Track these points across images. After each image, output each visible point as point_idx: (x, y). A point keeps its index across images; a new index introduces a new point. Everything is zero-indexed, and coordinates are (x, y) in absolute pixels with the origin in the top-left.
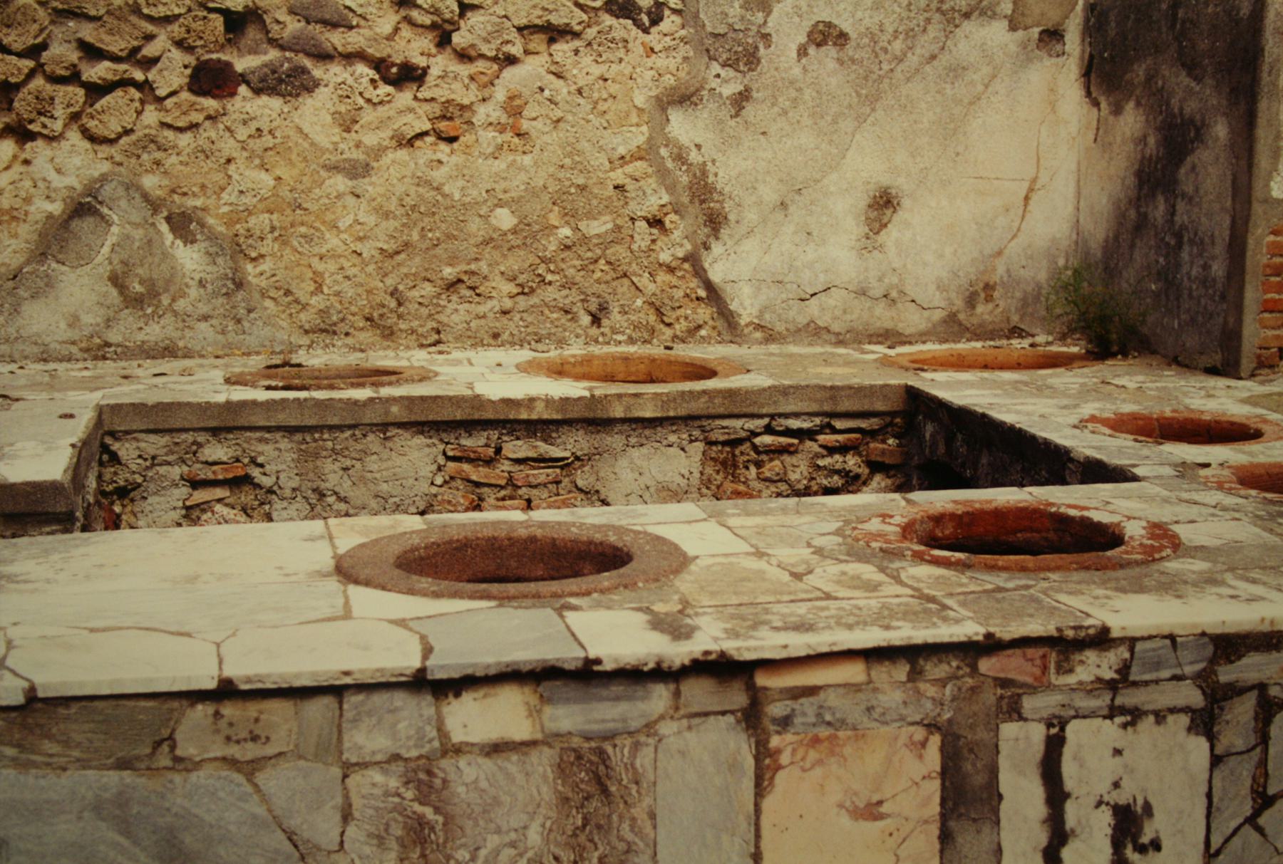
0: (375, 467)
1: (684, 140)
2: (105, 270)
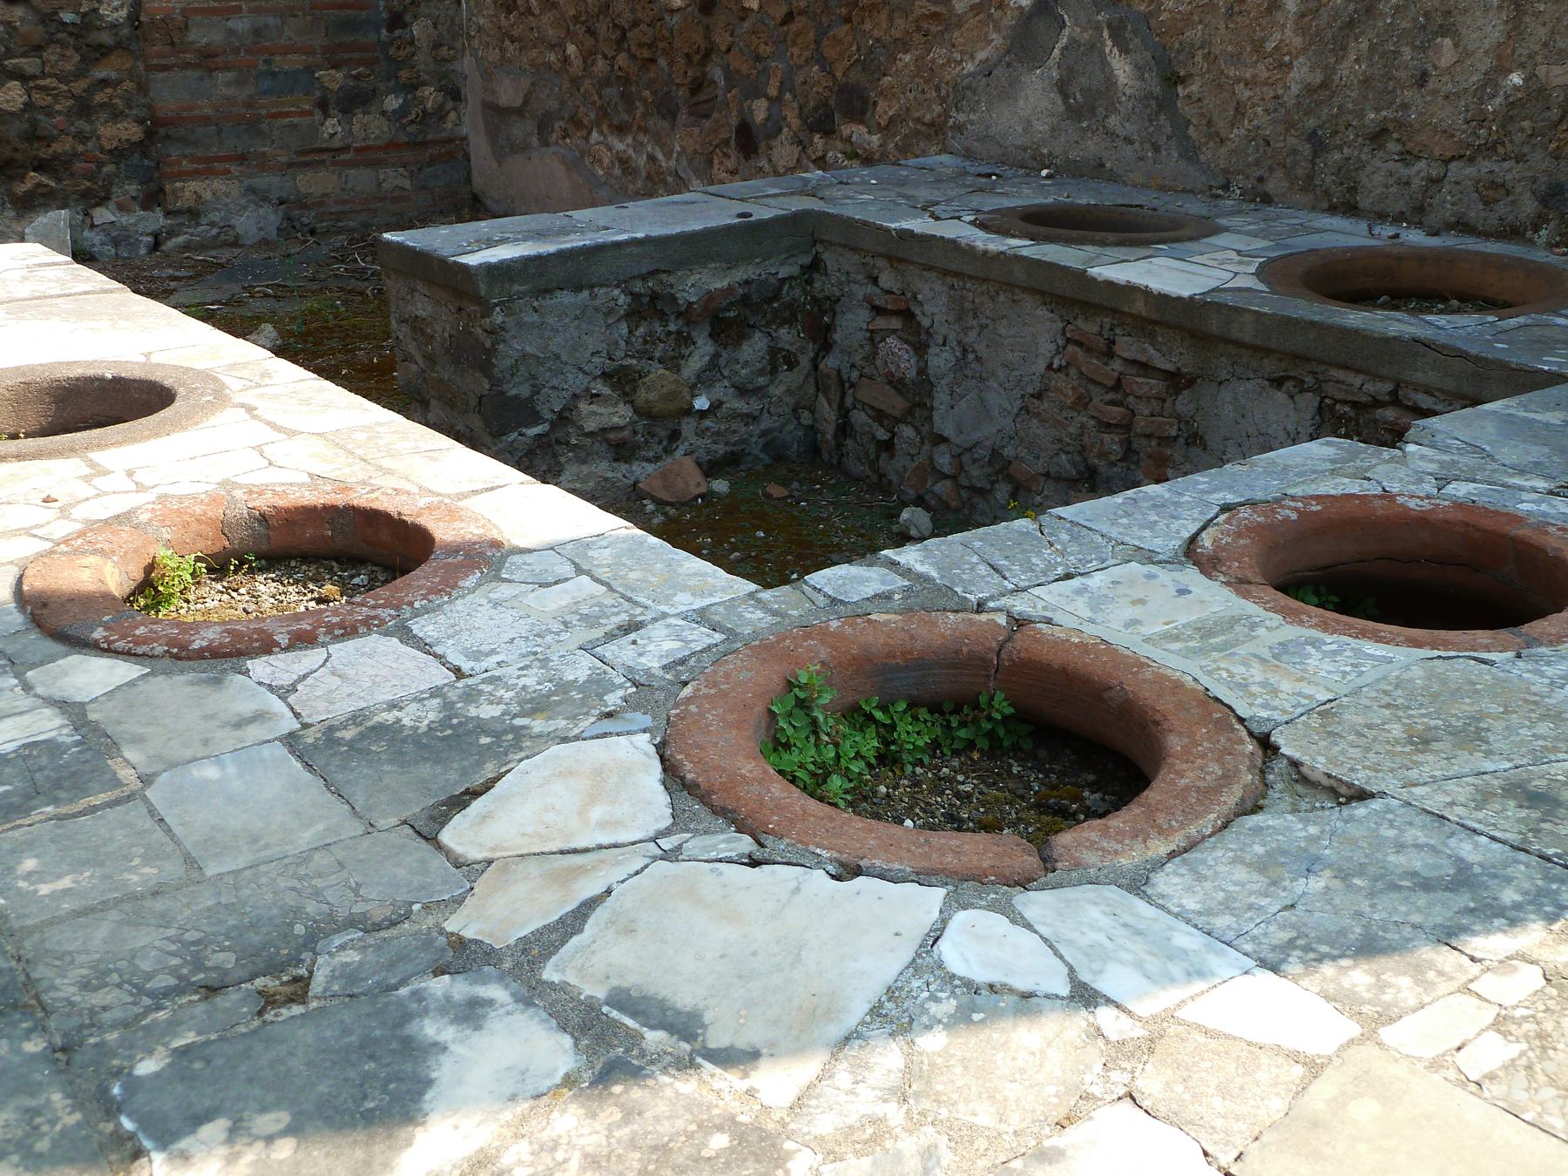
0: (1002, 331)
2: (1055, 74)
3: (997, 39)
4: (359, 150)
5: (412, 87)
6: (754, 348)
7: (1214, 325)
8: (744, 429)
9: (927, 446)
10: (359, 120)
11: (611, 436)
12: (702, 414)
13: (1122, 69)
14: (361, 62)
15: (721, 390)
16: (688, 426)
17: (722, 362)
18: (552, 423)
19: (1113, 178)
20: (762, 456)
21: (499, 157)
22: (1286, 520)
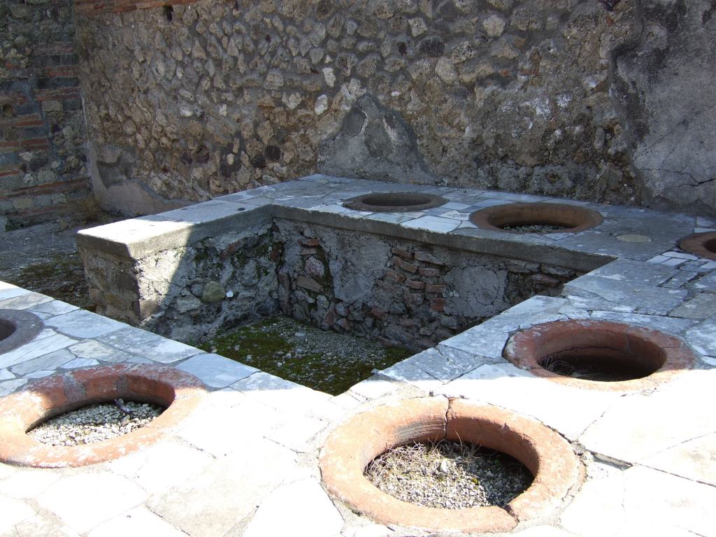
0: (363, 252)
1: (626, 79)
2: (363, 138)
3: (337, 125)
4: (41, 187)
5: (64, 157)
6: (250, 267)
7: (459, 244)
8: (248, 304)
9: (333, 304)
10: (40, 174)
11: (192, 313)
12: (231, 299)
13: (392, 134)
14: (41, 147)
15: (238, 287)
16: (225, 305)
17: (237, 275)
18: (166, 311)
19: (394, 181)
20: (257, 314)
21: (107, 186)
22: (537, 337)
